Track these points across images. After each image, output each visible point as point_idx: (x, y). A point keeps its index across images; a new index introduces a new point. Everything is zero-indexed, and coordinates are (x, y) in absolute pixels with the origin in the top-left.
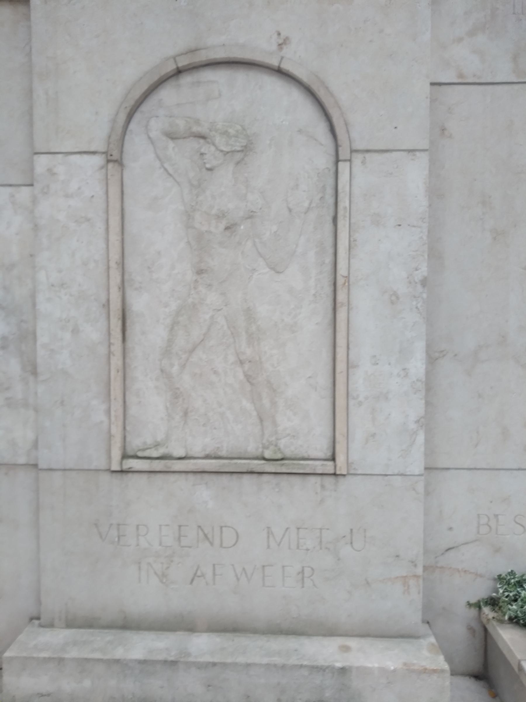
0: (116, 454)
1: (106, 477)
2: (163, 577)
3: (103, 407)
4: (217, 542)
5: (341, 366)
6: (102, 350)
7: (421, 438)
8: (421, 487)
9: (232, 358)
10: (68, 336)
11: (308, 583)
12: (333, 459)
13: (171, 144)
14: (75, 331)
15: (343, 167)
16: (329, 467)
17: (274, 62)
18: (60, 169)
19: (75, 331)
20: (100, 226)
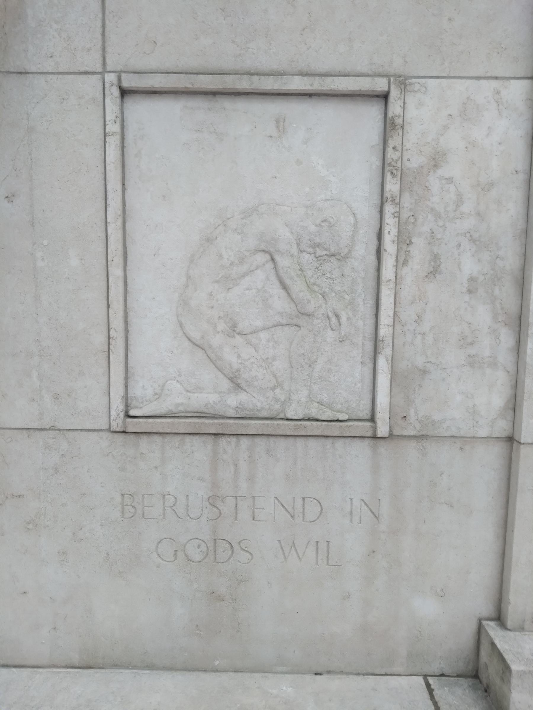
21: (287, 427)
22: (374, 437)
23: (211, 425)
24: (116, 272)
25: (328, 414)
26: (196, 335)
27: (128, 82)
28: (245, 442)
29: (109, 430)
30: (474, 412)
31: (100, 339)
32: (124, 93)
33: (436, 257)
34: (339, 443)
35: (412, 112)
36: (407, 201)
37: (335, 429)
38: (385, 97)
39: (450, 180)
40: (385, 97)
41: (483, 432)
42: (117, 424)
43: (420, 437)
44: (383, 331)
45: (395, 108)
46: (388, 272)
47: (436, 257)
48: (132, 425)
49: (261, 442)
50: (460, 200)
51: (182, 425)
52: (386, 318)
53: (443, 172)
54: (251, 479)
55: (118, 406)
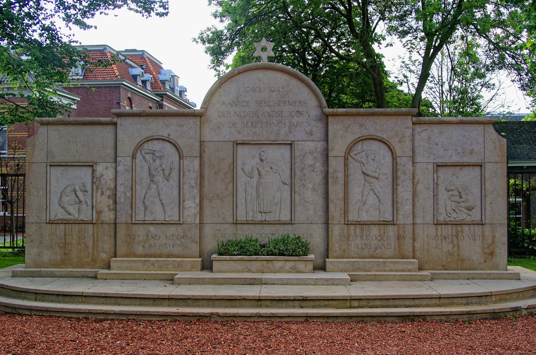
1: (131, 225)
2: (143, 247)
3: (131, 210)
4: (155, 239)
5: (181, 201)
6: (131, 198)
7: (198, 216)
8: (198, 226)
9: (159, 199)
10: (123, 195)
11: (175, 247)
12: (180, 221)
13: (146, 155)
14: (125, 194)
15: (182, 161)
16: (179, 222)
17: (167, 139)
18: (122, 160)
19: (125, 194)
20: (131, 172)
21: (77, 222)
22: (93, 223)
23: (64, 222)
24: (48, 195)
26: (62, 206)
27: (51, 164)
29: (46, 223)
30: (110, 219)
31: (45, 207)
32: (50, 166)
33: (102, 192)
35: (97, 168)
36: (97, 182)
38: (92, 166)
39: (104, 179)
40: (92, 166)
41: (112, 222)
43: (101, 223)
44: (94, 204)
45: (95, 168)
46: (94, 194)
48: (51, 222)
50: (106, 183)
51: (60, 222)
52: (94, 202)
53: (103, 178)
54: (72, 232)
55: (48, 218)
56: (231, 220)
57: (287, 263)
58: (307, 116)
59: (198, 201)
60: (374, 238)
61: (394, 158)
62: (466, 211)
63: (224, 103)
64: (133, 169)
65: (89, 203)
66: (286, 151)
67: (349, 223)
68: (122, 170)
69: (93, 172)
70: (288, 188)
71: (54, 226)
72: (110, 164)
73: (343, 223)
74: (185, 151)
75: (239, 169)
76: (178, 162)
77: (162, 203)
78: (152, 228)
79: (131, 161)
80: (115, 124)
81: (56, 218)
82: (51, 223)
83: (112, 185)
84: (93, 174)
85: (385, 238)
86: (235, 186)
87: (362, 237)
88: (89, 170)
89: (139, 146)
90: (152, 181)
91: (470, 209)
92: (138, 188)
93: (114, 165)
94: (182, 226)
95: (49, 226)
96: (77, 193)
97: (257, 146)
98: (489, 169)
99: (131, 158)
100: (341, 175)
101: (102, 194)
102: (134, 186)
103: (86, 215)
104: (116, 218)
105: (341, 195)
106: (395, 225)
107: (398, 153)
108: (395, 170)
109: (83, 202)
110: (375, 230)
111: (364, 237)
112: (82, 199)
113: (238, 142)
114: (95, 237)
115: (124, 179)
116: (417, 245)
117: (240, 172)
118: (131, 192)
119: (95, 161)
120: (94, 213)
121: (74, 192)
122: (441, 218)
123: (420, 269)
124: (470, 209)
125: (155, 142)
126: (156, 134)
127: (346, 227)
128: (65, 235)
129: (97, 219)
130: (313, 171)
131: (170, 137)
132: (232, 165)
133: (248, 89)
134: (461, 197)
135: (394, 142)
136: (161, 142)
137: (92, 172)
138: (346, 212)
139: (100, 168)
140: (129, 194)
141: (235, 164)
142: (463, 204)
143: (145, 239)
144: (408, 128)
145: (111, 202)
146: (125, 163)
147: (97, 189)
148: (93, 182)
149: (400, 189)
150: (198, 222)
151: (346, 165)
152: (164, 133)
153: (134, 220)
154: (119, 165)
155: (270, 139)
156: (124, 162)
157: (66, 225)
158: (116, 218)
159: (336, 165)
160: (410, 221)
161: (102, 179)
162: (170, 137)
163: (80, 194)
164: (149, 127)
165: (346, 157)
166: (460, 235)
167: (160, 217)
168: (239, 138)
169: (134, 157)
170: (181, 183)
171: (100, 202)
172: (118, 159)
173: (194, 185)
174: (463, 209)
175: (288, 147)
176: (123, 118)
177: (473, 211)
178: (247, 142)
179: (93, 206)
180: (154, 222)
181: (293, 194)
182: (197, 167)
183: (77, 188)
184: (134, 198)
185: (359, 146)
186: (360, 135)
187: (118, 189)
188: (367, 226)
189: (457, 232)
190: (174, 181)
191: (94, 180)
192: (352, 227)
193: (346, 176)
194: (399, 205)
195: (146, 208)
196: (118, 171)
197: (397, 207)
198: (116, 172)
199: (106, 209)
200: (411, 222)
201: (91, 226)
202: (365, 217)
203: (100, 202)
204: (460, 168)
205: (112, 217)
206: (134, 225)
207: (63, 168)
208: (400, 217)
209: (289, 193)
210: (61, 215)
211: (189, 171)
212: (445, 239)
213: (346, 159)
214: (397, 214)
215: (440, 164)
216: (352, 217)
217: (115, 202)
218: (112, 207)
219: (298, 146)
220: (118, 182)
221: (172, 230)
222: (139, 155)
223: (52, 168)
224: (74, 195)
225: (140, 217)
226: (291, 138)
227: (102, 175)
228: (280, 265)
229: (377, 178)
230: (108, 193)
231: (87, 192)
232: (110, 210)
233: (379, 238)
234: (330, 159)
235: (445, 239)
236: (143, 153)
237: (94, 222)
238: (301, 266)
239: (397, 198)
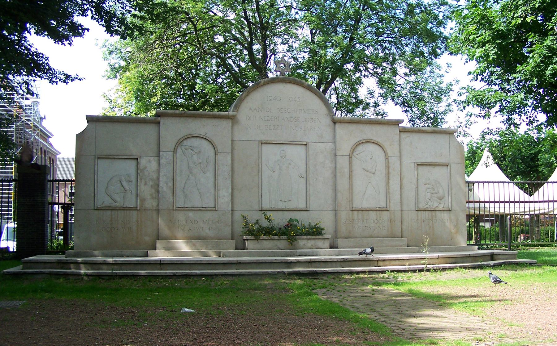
0: (175, 207)
6: (172, 187)
8: (231, 212)
14: (167, 184)
16: (214, 209)
17: (204, 137)
18: (165, 154)
19: (167, 184)
20: (172, 165)
21: (123, 209)
23: (111, 208)
25: (130, 206)
28: (116, 211)
30: (153, 206)
31: (93, 195)
32: (98, 158)
33: (146, 182)
34: (132, 211)
36: (141, 174)
37: (131, 209)
42: (96, 209)
44: (138, 193)
46: (139, 184)
47: (146, 182)
48: (98, 209)
49: (119, 211)
51: (107, 208)
52: (138, 191)
53: (146, 169)
54: (117, 217)
56: (257, 208)
57: (309, 241)
58: (319, 122)
59: (230, 190)
60: (372, 221)
61: (387, 158)
62: (438, 200)
63: (251, 109)
64: (174, 162)
65: (134, 192)
66: (302, 149)
67: (353, 209)
68: (165, 163)
69: (138, 164)
70: (303, 181)
71: (101, 212)
72: (152, 158)
73: (349, 209)
74: (219, 149)
75: (264, 164)
76: (214, 157)
77: (200, 193)
78: (191, 214)
79: (173, 155)
80: (159, 123)
81: (103, 206)
82: (98, 209)
83: (155, 176)
84: (137, 166)
85: (381, 221)
86: (260, 179)
87: (363, 221)
88: (134, 163)
89: (180, 143)
90: (191, 173)
91: (441, 199)
92: (178, 178)
93: (156, 158)
94: (217, 212)
95: (96, 212)
96: (122, 182)
97: (278, 146)
98: (453, 166)
99: (172, 153)
100: (347, 170)
101: (146, 184)
102: (175, 177)
103: (130, 202)
104: (158, 205)
105: (347, 186)
106: (388, 212)
107: (390, 154)
108: (388, 167)
109: (128, 191)
110: (373, 214)
111: (365, 221)
112: (127, 188)
113: (263, 142)
114: (139, 222)
115: (166, 171)
116: (404, 227)
117: (264, 168)
118: (172, 182)
119: (139, 154)
120: (139, 201)
121: (119, 182)
122: (421, 206)
123: (408, 247)
124: (441, 199)
125: (193, 140)
126: (195, 133)
127: (351, 212)
128: (111, 221)
129: (141, 206)
130: (324, 167)
131: (206, 135)
132: (258, 161)
133: (271, 98)
134: (434, 190)
135: (386, 145)
136: (198, 139)
137: (136, 165)
138: (351, 201)
139: (143, 162)
140: (170, 184)
141: (260, 160)
142: (436, 195)
143: (184, 223)
144: (396, 134)
145: (153, 191)
146: (167, 157)
147: (141, 179)
148: (137, 174)
149: (391, 182)
150: (230, 209)
151: (350, 162)
152: (202, 132)
153: (175, 207)
154: (162, 158)
155: (289, 140)
156: (167, 156)
157: (113, 212)
158: (158, 205)
159: (343, 162)
160: (398, 207)
161: (145, 171)
162: (206, 135)
163: (125, 184)
164: (188, 126)
165: (351, 156)
166: (434, 218)
167: (197, 204)
168: (264, 138)
169: (175, 152)
170: (216, 175)
171: (144, 191)
172: (161, 153)
173: (227, 177)
174: (436, 199)
175: (304, 147)
176: (166, 118)
177: (443, 200)
178: (270, 142)
179: (137, 194)
180: (193, 209)
181: (308, 185)
182: (230, 162)
183: (123, 179)
184: (175, 187)
185: (360, 148)
186: (361, 139)
187: (161, 179)
188: (367, 212)
189: (432, 216)
190: (210, 175)
191: (139, 172)
192: (356, 213)
193: (351, 171)
194: (391, 195)
195: (185, 196)
196: (161, 164)
197: (389, 197)
198: (159, 165)
199: (149, 197)
200: (400, 209)
201: (135, 213)
202: (365, 205)
203: (144, 191)
204: (433, 167)
205: (155, 204)
206: (175, 211)
207: (109, 160)
208: (391, 204)
209: (305, 185)
210: (108, 202)
211: (223, 164)
212: (424, 222)
213: (350, 158)
214: (390, 202)
215: (419, 164)
216: (357, 204)
217: (158, 192)
218: (154, 195)
219: (312, 146)
220: (160, 174)
221: (208, 215)
222: (179, 151)
223: (99, 160)
224: (119, 184)
225: (180, 204)
226: (305, 140)
227: (146, 167)
228: (304, 243)
229: (374, 174)
230: (151, 183)
231: (131, 182)
232: (153, 198)
233: (376, 221)
234: (338, 158)
235: (424, 222)
236: (183, 149)
237: (138, 209)
238: (320, 243)
239: (389, 189)
